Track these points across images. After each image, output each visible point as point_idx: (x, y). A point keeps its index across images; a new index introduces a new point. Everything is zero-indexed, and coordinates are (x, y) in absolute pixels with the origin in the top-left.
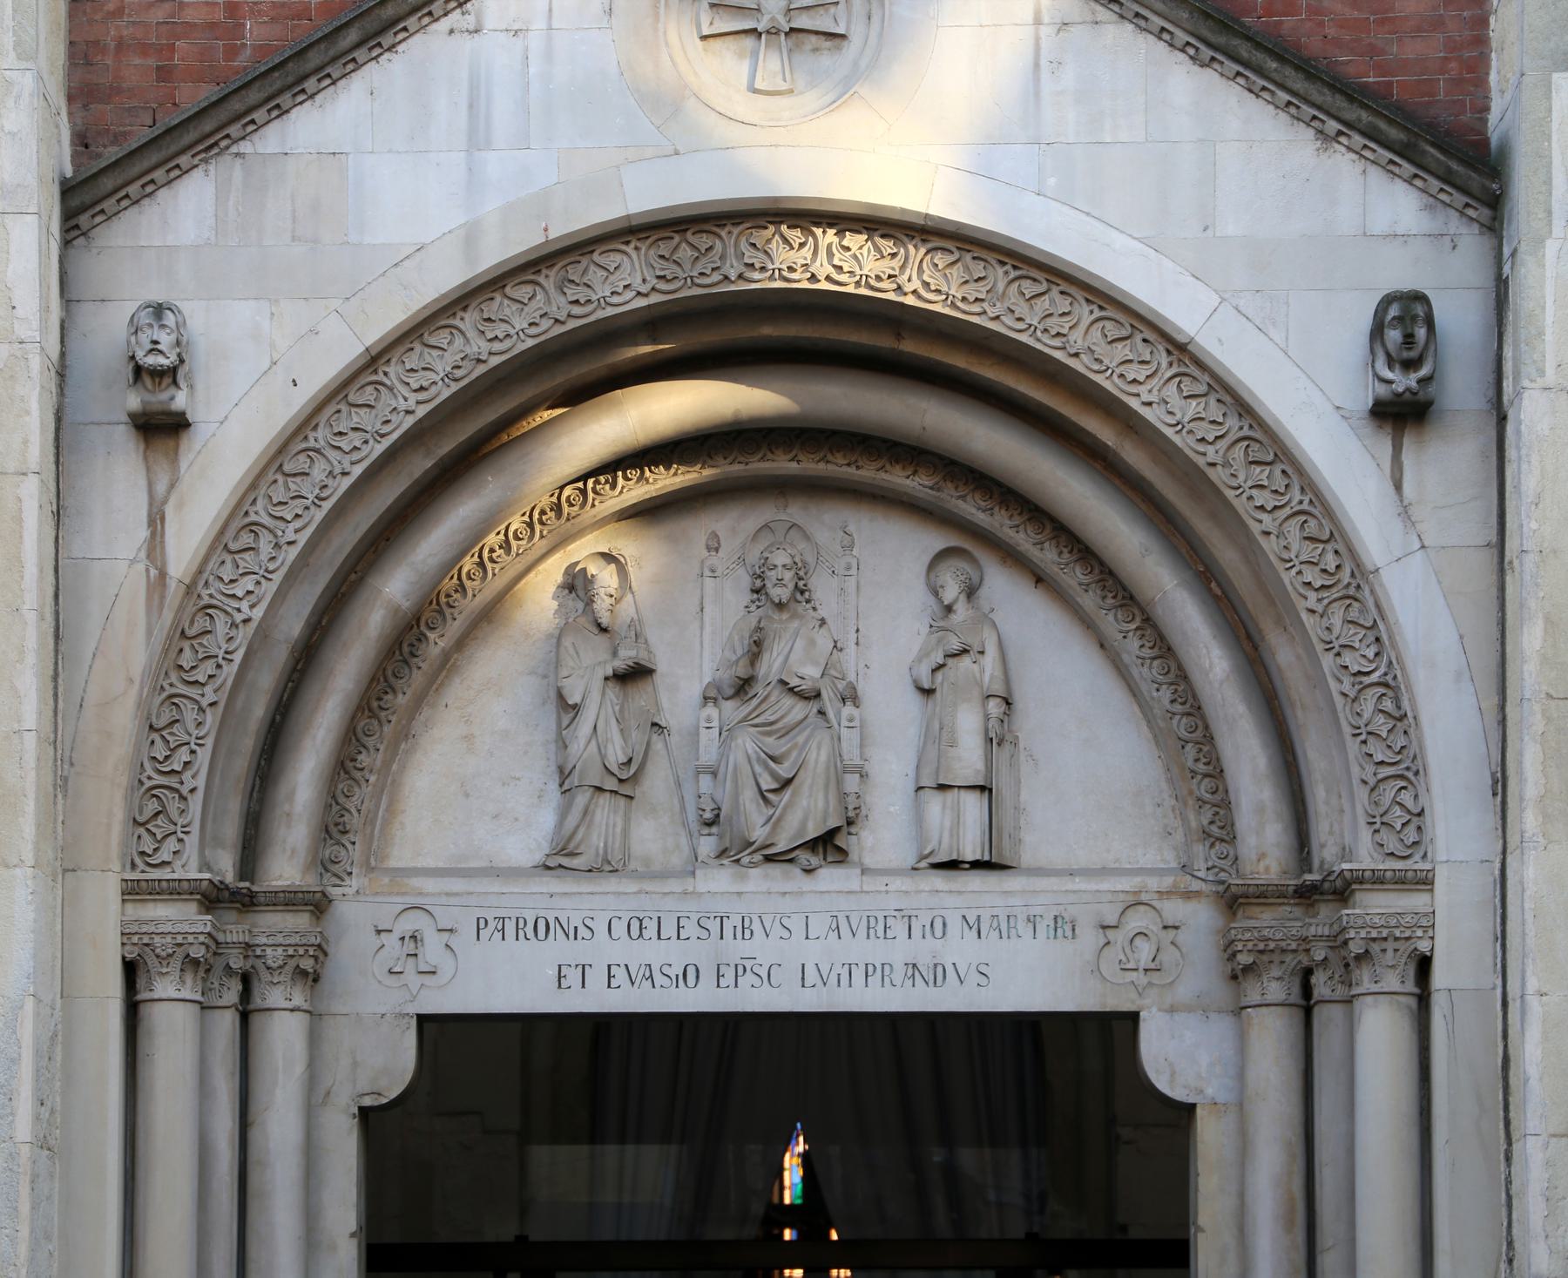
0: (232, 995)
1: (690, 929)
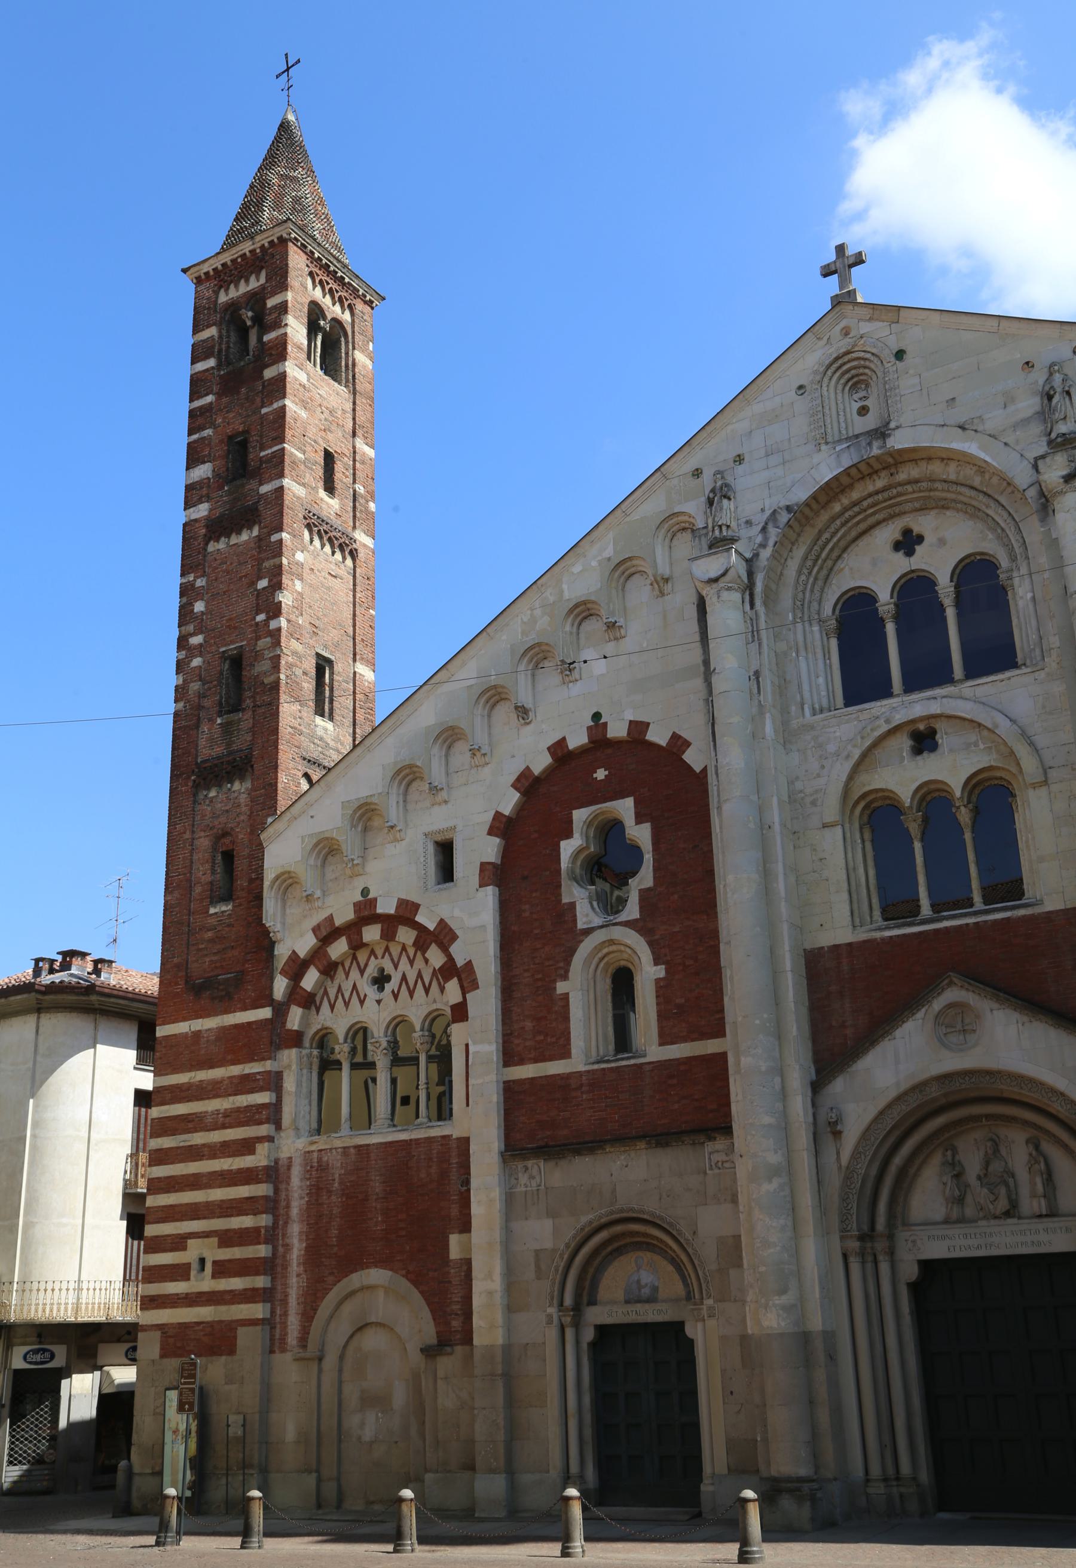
0: (870, 1258)
1: (978, 1236)
